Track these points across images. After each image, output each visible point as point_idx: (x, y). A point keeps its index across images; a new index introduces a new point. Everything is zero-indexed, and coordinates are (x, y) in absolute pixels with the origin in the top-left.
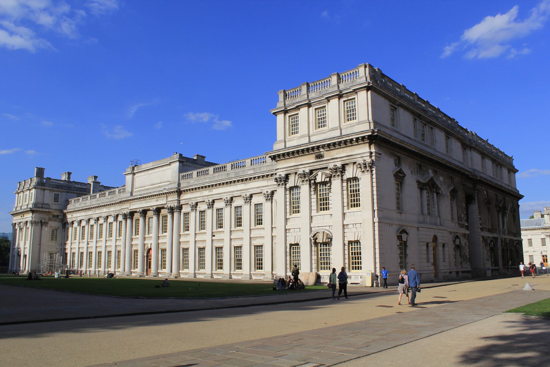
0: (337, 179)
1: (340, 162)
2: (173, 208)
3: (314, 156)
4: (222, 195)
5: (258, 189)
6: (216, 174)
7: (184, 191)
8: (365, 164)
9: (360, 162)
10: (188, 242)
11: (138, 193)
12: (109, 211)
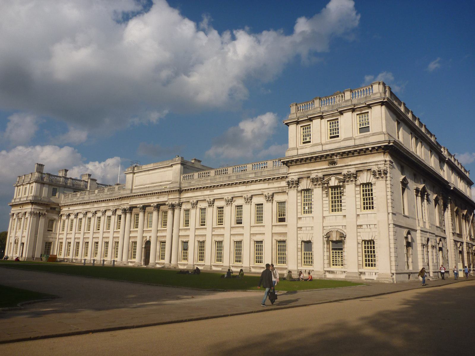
0: (351, 184)
1: (354, 169)
2: (174, 204)
3: (327, 162)
4: (222, 195)
5: (260, 191)
6: (218, 177)
7: (186, 190)
8: (380, 171)
9: (375, 169)
10: (165, 236)
11: (138, 191)
12: (108, 205)
